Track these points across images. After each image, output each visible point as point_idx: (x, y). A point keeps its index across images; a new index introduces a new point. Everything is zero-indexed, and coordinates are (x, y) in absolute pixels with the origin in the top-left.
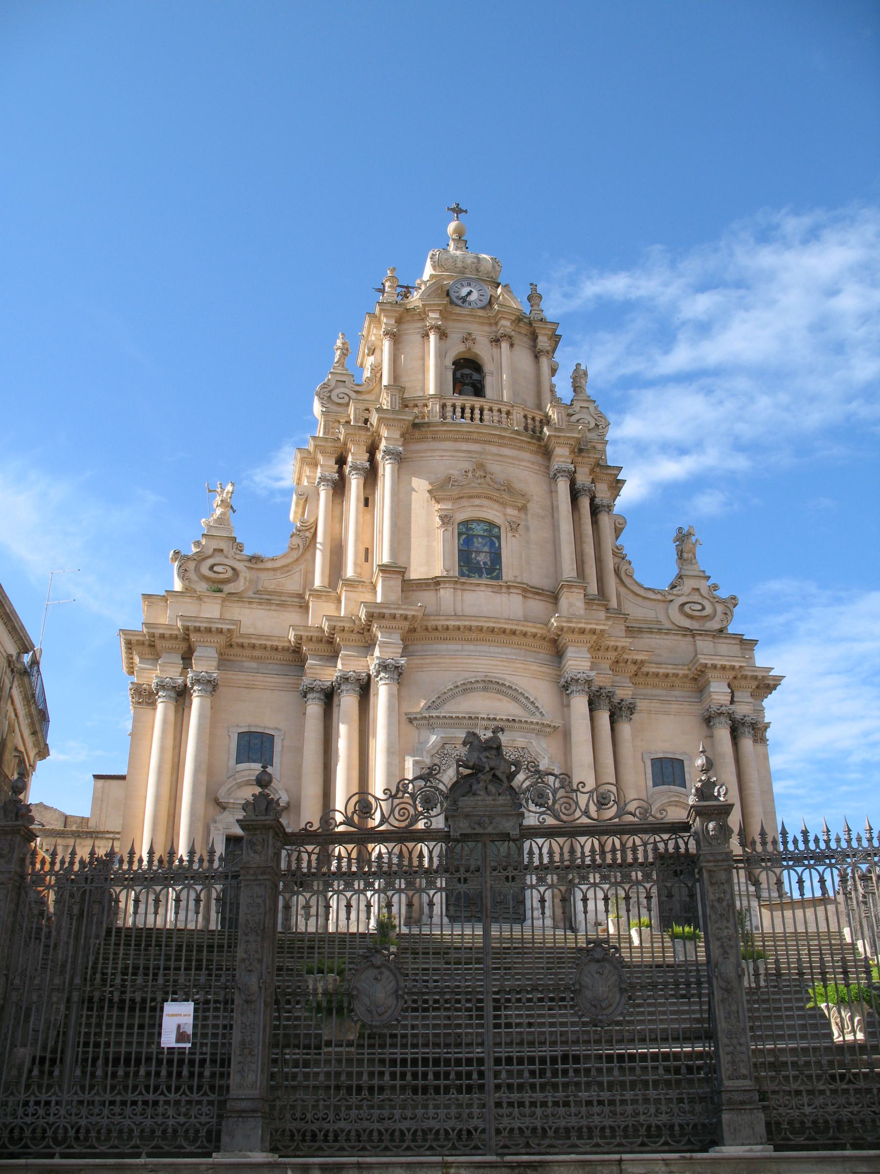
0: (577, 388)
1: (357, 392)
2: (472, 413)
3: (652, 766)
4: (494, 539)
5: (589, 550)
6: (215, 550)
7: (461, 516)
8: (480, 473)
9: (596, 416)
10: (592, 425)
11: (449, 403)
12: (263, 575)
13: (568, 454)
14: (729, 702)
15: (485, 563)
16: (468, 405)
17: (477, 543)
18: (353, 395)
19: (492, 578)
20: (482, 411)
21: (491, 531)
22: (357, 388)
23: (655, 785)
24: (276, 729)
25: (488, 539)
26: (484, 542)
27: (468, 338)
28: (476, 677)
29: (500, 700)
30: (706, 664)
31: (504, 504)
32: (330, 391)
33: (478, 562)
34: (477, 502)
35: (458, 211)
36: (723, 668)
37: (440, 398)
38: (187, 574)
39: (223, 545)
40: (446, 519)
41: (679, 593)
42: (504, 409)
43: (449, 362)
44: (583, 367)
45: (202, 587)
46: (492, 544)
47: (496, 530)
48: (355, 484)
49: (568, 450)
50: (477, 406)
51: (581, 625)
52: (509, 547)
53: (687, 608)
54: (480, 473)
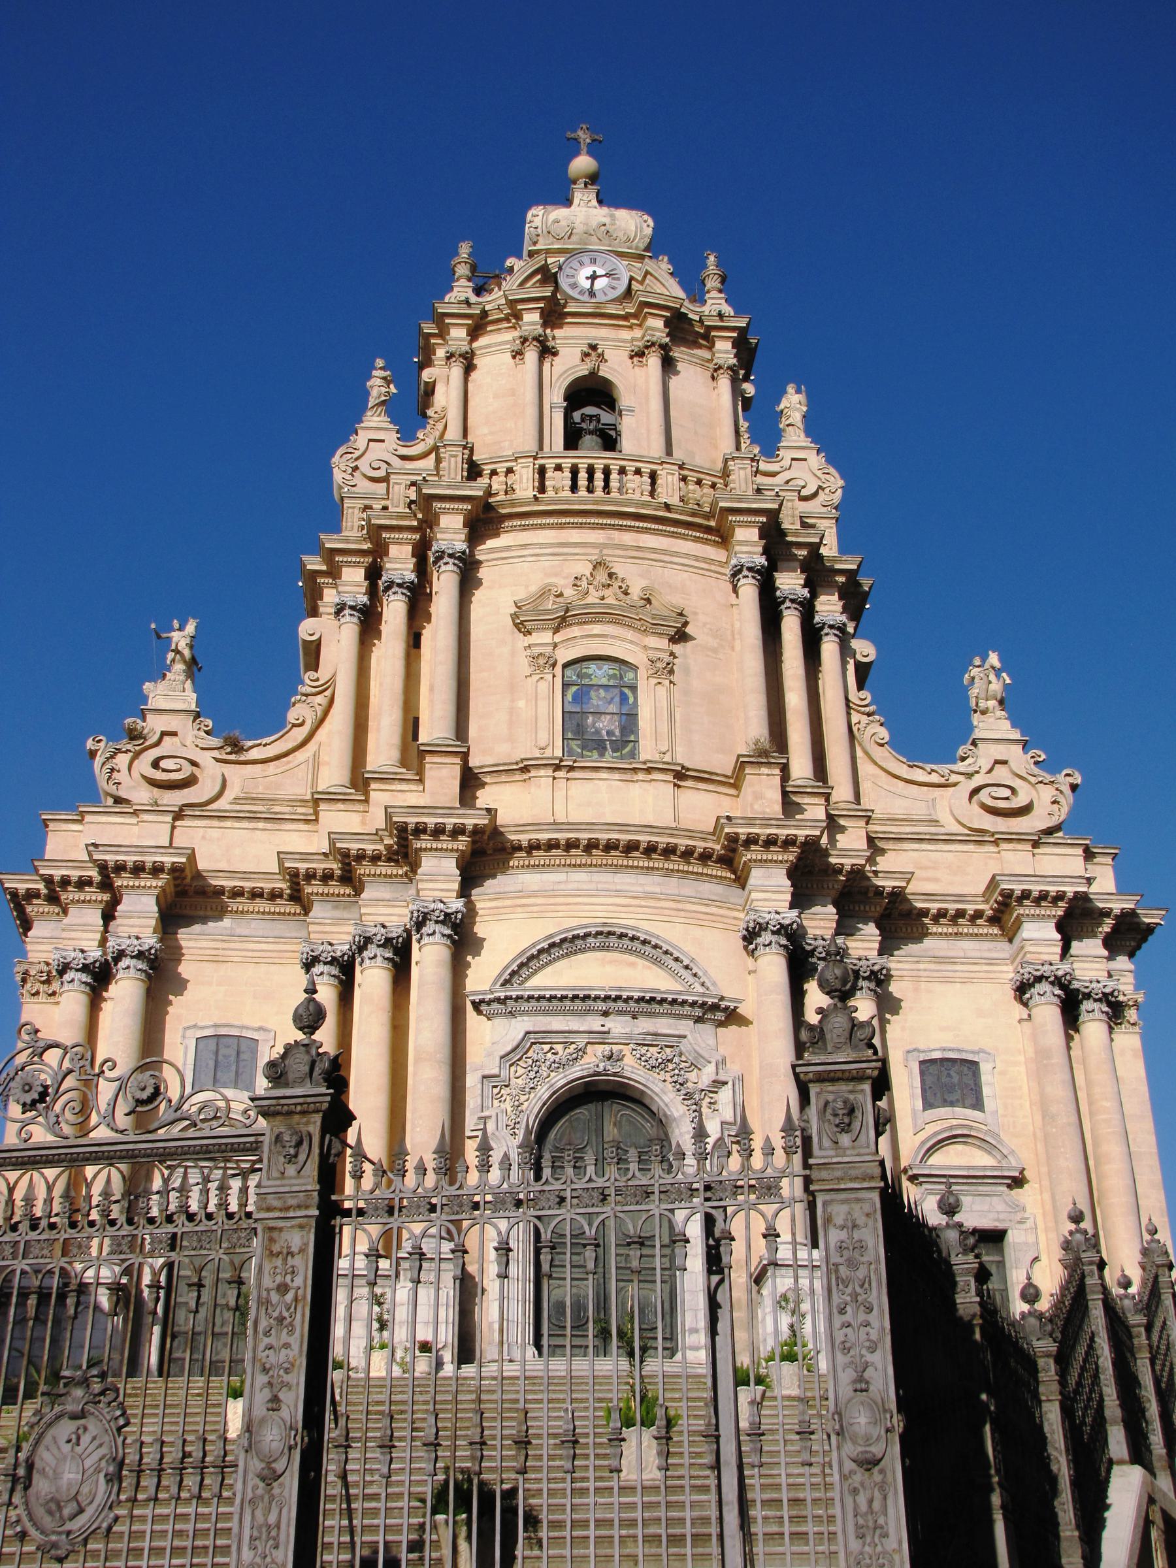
1: (404, 458)
2: (591, 479)
3: (922, 1073)
4: (626, 690)
6: (163, 734)
7: (565, 655)
9: (819, 473)
11: (550, 464)
13: (756, 538)
14: (1058, 957)
15: (609, 733)
16: (583, 466)
17: (597, 699)
18: (396, 462)
19: (622, 757)
20: (607, 472)
21: (621, 678)
23: (928, 1105)
24: (261, 1029)
25: (616, 691)
26: (609, 697)
28: (586, 926)
29: (633, 965)
30: (1012, 891)
32: (357, 459)
33: (598, 732)
34: (597, 629)
36: (1043, 896)
37: (535, 458)
38: (115, 774)
41: (971, 770)
42: (646, 468)
43: (556, 397)
46: (624, 698)
47: (631, 675)
48: (394, 610)
49: (756, 531)
50: (599, 465)
51: (768, 831)
53: (984, 796)
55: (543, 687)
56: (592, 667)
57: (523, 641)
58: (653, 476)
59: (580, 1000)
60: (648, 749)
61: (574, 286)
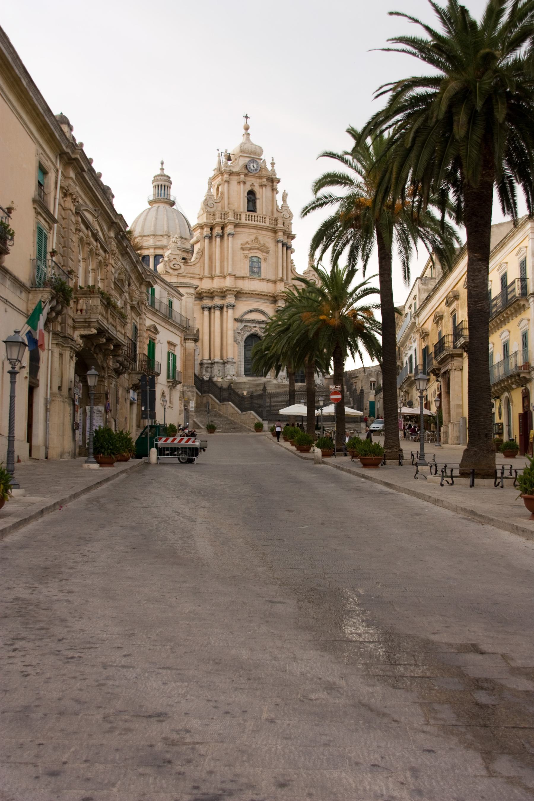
0: (284, 200)
5: (285, 265)
8: (256, 241)
10: (288, 217)
12: (188, 267)
18: (214, 203)
22: (216, 201)
27: (252, 185)
31: (262, 251)
34: (255, 251)
35: (247, 117)
39: (175, 257)
40: (246, 257)
43: (246, 194)
44: (286, 192)
45: (171, 271)
52: (263, 265)
54: (256, 241)
55: (246, 262)
56: (254, 258)
57: (243, 252)
58: (265, 218)
59: (253, 321)
60: (263, 277)
61: (250, 168)
